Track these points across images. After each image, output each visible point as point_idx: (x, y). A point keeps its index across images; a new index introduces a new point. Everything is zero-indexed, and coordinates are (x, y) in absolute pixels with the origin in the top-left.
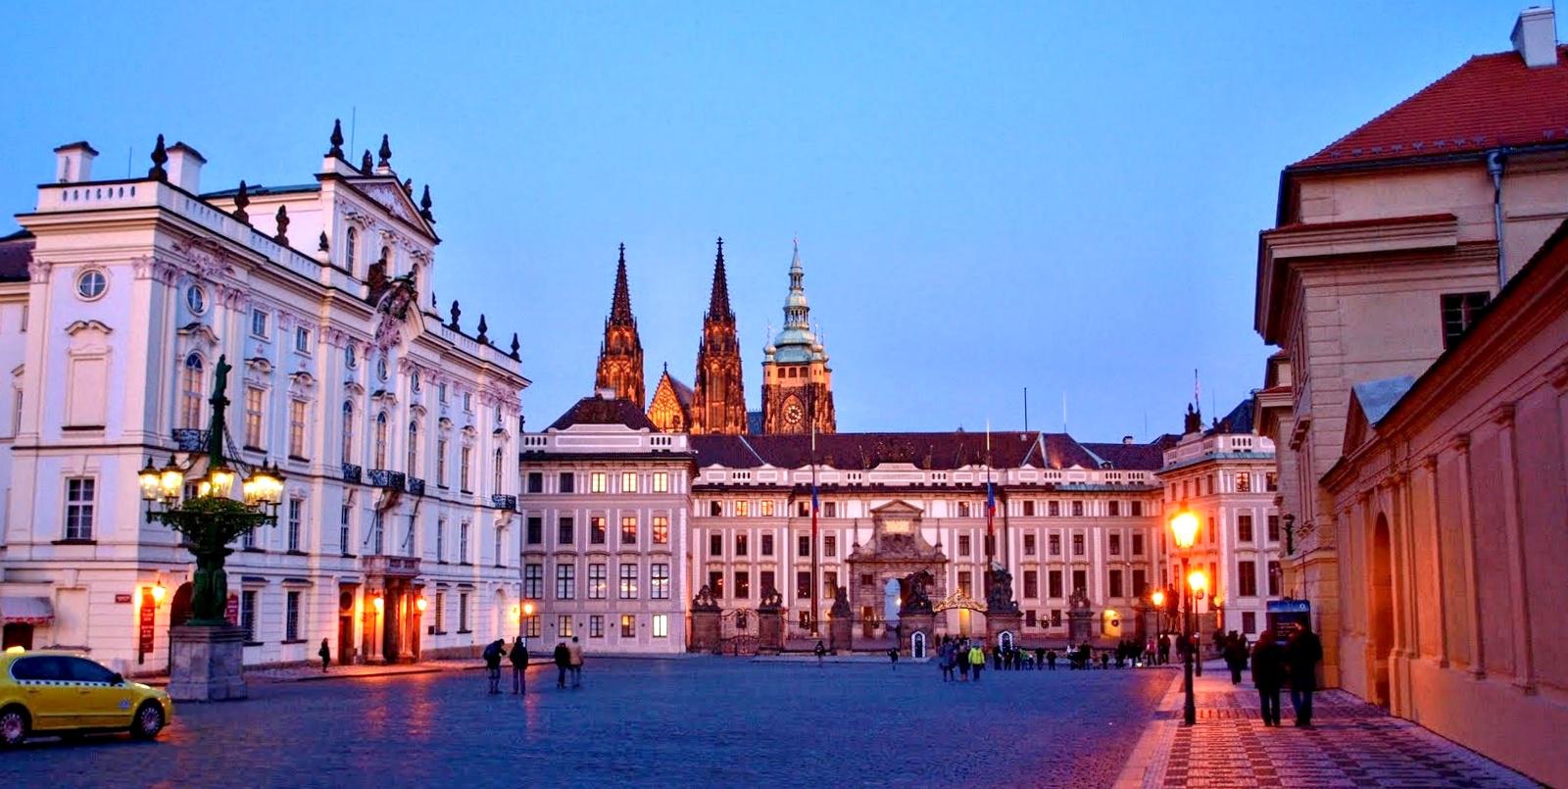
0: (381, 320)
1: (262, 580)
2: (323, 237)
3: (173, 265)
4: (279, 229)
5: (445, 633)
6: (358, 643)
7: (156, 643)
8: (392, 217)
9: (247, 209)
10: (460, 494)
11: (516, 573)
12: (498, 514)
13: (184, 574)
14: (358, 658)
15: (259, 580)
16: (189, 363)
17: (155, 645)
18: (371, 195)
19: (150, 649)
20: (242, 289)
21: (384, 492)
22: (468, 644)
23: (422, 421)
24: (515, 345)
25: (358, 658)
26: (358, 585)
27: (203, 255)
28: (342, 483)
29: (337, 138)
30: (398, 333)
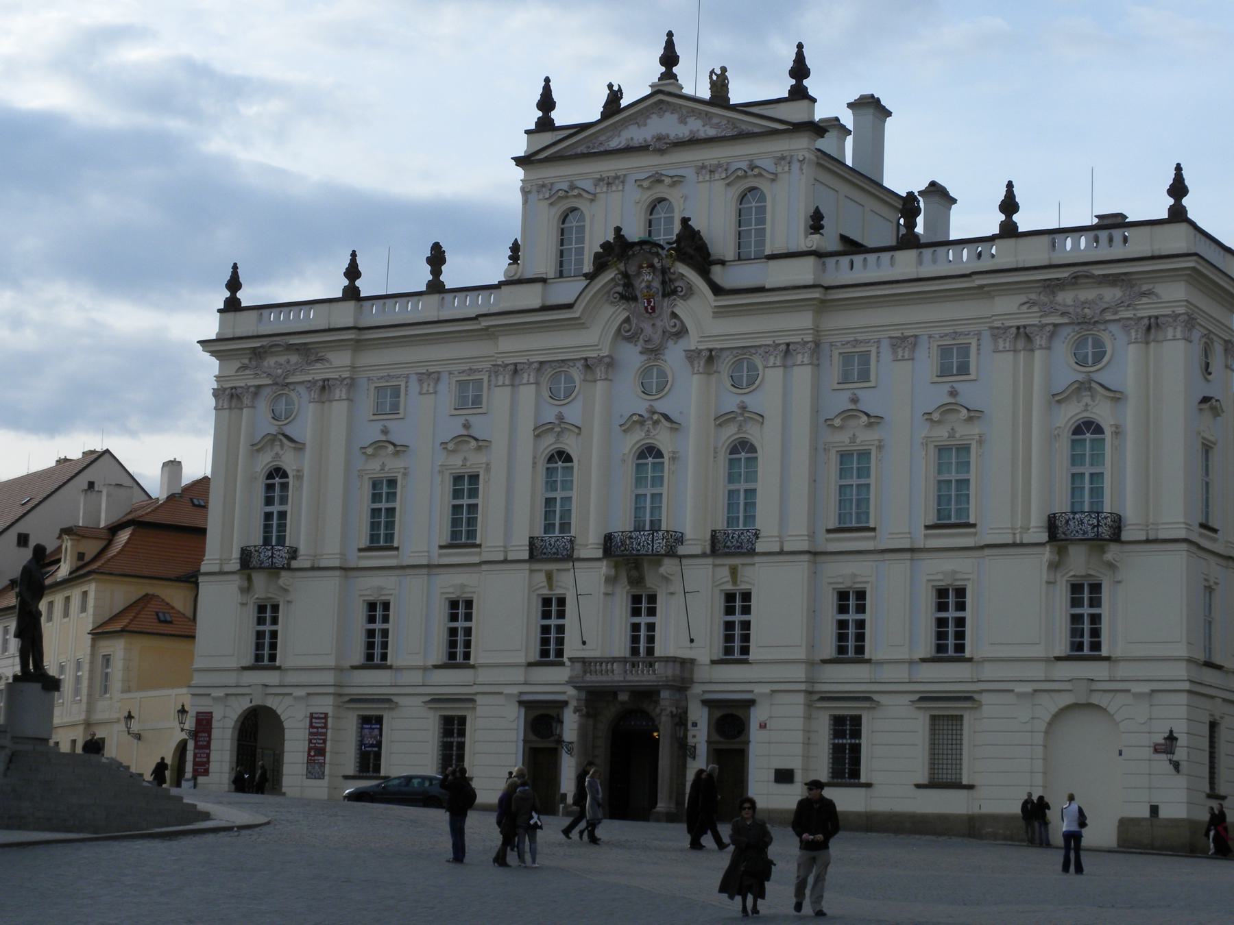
0: (625, 314)
1: (389, 701)
2: (515, 248)
3: (235, 388)
4: (432, 272)
5: (868, 785)
6: (568, 785)
7: (213, 767)
8: (661, 152)
9: (358, 283)
10: (923, 531)
11: (1181, 671)
12: (1047, 554)
13: (248, 699)
14: (566, 806)
15: (387, 700)
16: (270, 476)
17: (211, 770)
18: (614, 144)
19: (206, 773)
20: (335, 376)
21: (616, 567)
22: (975, 810)
23: (766, 440)
24: (1178, 189)
25: (566, 806)
26: (565, 703)
27: (282, 359)
28: (526, 566)
29: (546, 103)
30: (674, 315)
